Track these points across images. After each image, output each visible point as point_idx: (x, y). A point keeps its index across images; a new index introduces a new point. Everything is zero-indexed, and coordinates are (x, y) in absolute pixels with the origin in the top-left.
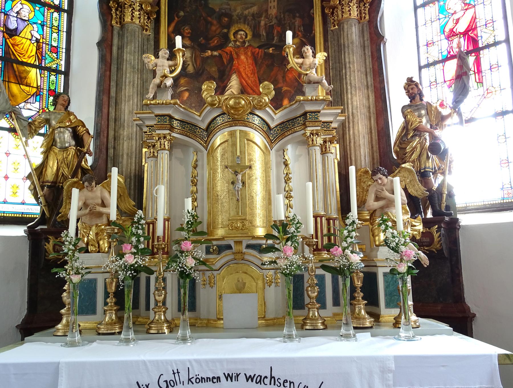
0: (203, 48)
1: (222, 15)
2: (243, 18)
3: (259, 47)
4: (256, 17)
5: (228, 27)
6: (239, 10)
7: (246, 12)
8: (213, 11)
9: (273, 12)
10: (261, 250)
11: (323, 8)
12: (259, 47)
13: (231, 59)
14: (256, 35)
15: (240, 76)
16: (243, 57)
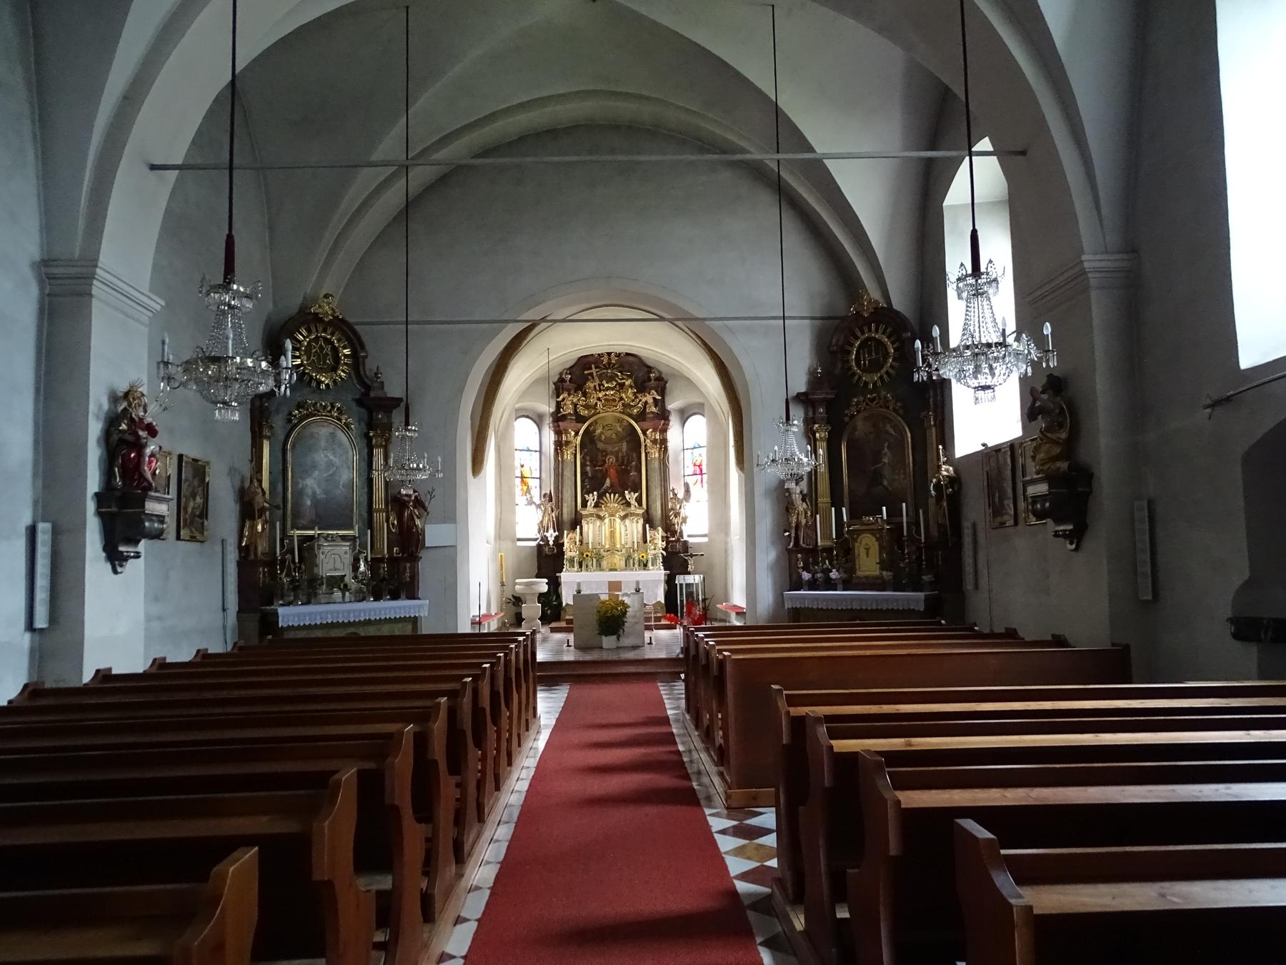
0: (595, 467)
1: (602, 451)
2: (612, 453)
3: (619, 465)
4: (618, 452)
5: (605, 456)
6: (610, 449)
7: (613, 450)
8: (598, 449)
9: (624, 450)
10: (618, 551)
11: (645, 450)
12: (619, 465)
13: (607, 471)
14: (617, 460)
15: (610, 479)
16: (611, 470)
